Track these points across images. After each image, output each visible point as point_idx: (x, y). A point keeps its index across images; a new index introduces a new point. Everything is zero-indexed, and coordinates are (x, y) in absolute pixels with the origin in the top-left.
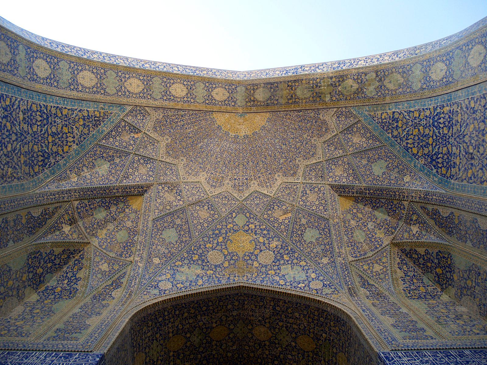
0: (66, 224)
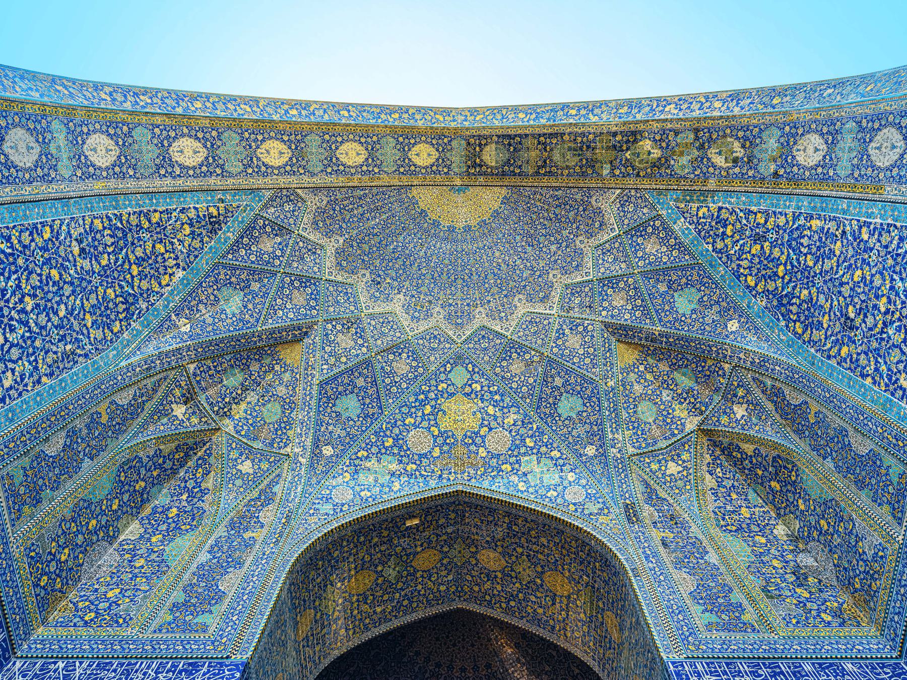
0: (177, 403)
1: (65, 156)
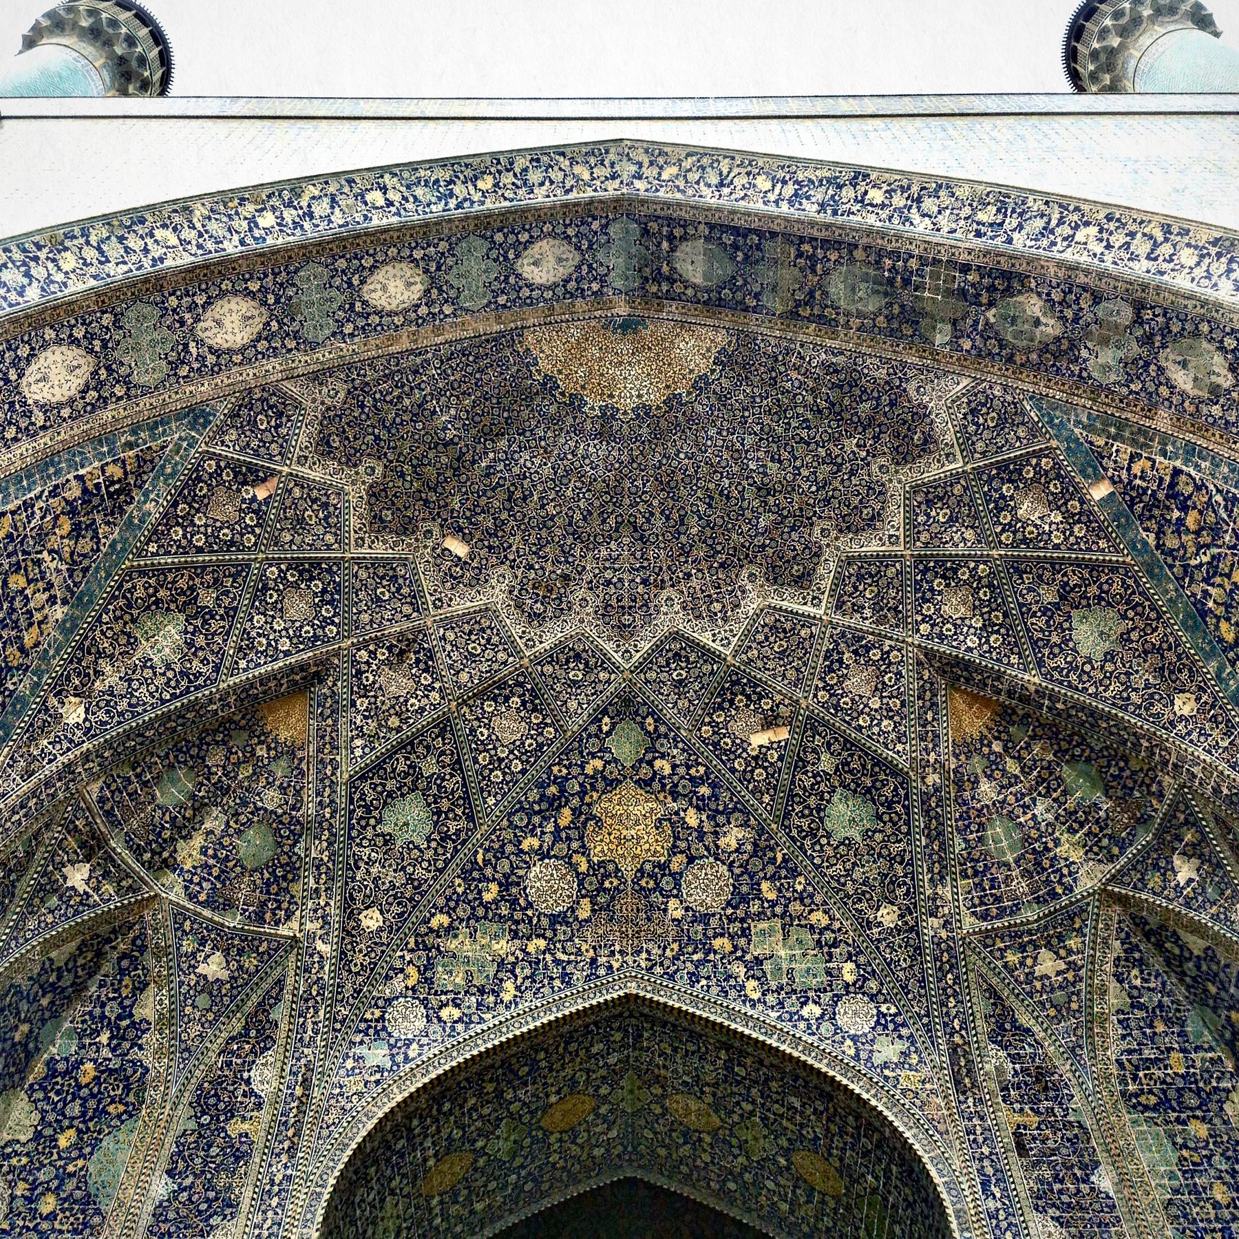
0: (72, 863)
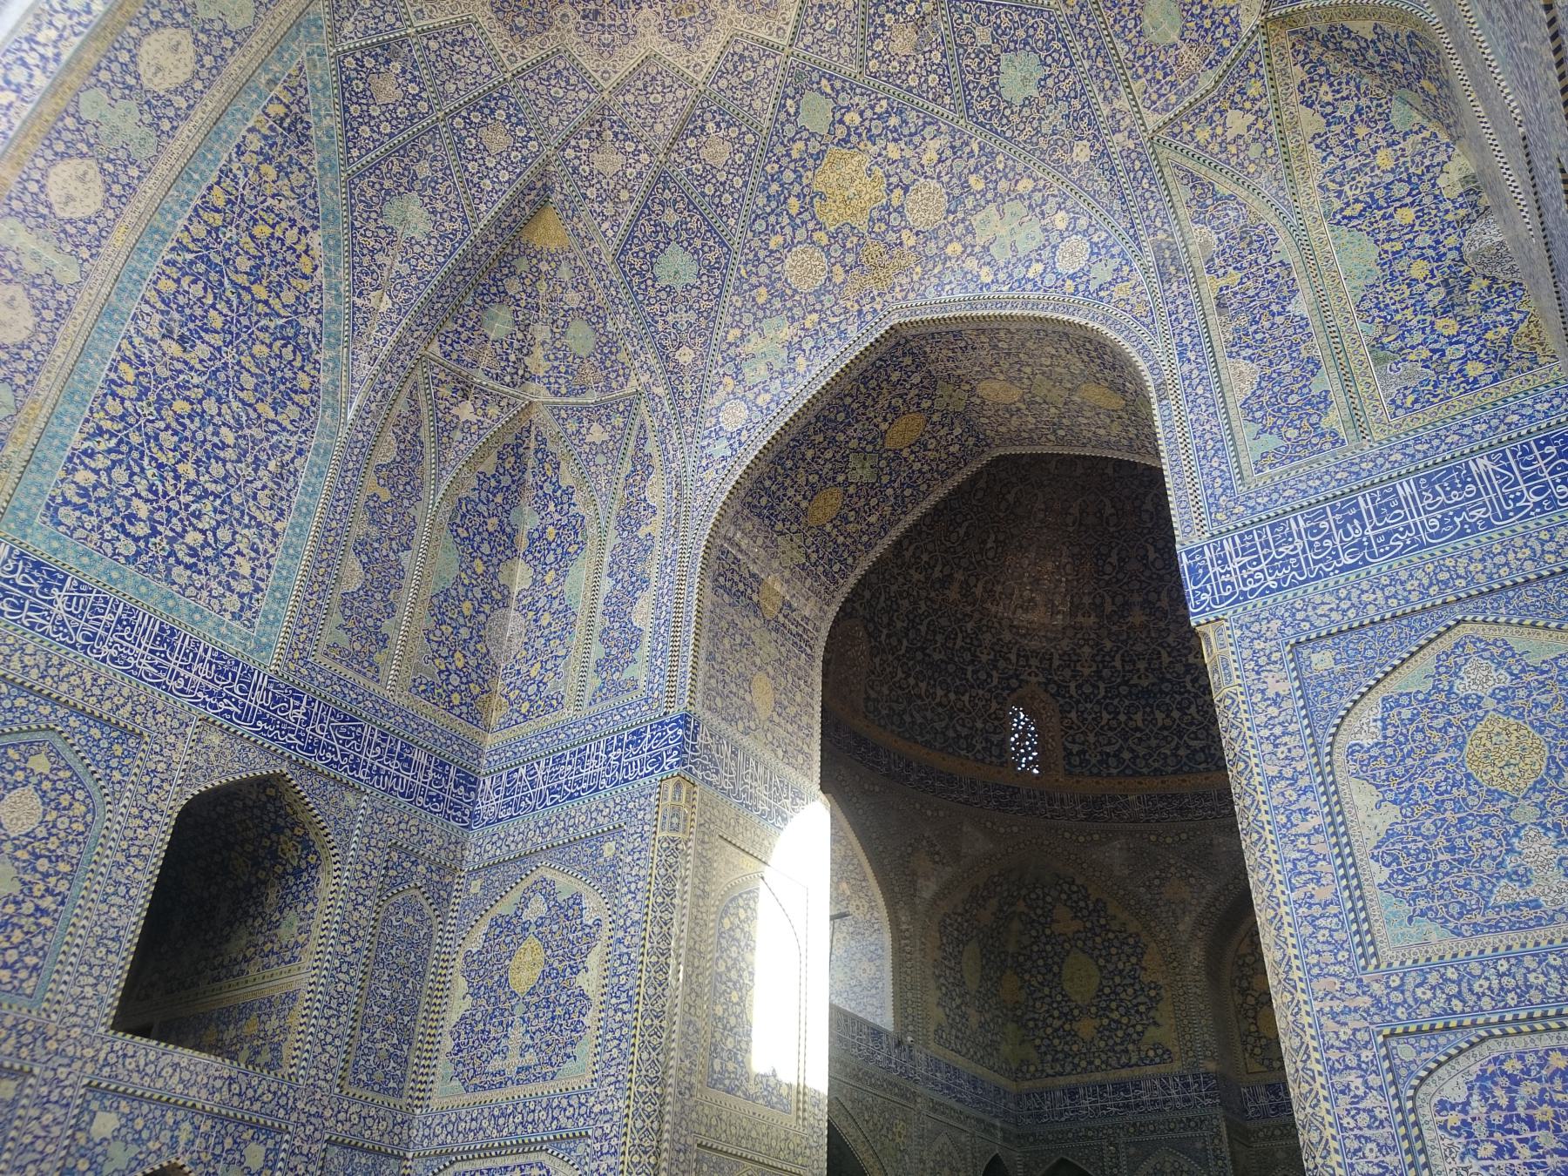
1: (49, 255)
